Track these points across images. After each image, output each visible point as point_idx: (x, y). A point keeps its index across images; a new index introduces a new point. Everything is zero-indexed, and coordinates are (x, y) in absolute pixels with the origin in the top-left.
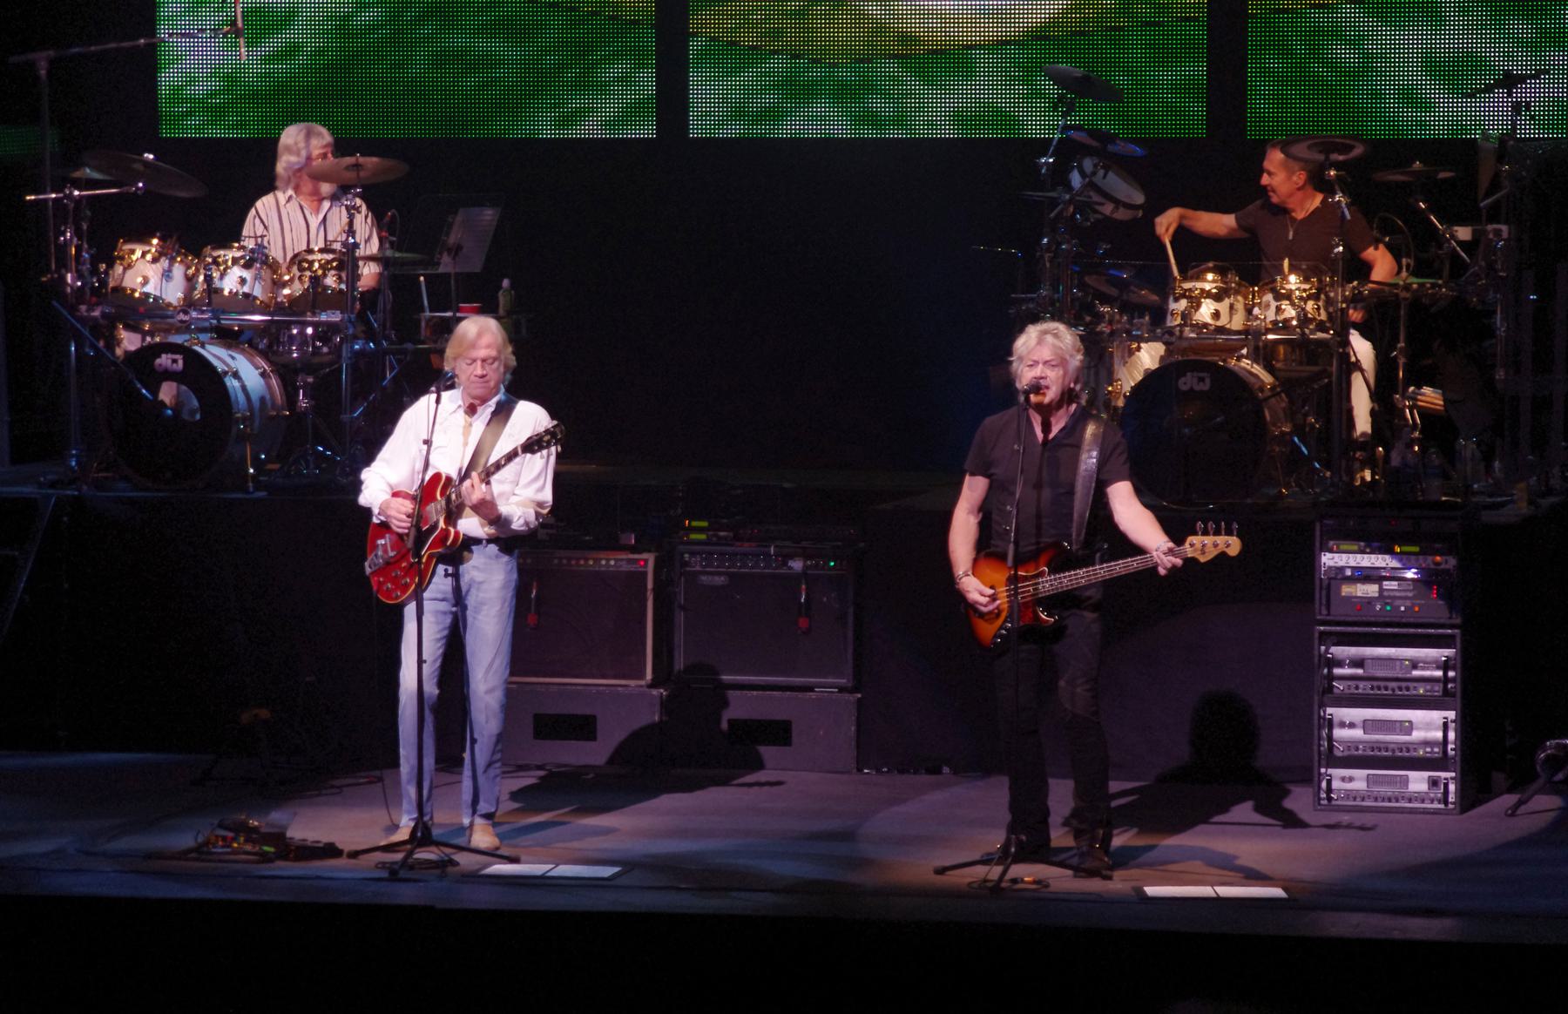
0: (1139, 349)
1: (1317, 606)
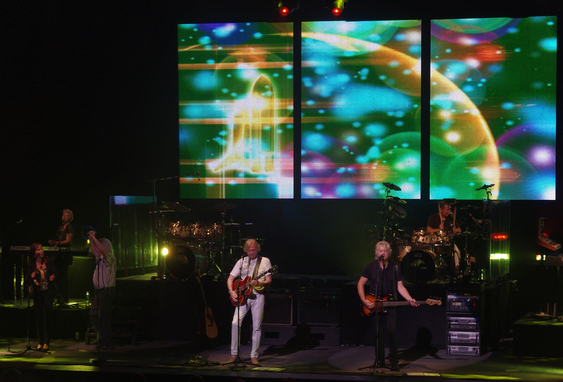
0: (405, 248)
1: (447, 308)
